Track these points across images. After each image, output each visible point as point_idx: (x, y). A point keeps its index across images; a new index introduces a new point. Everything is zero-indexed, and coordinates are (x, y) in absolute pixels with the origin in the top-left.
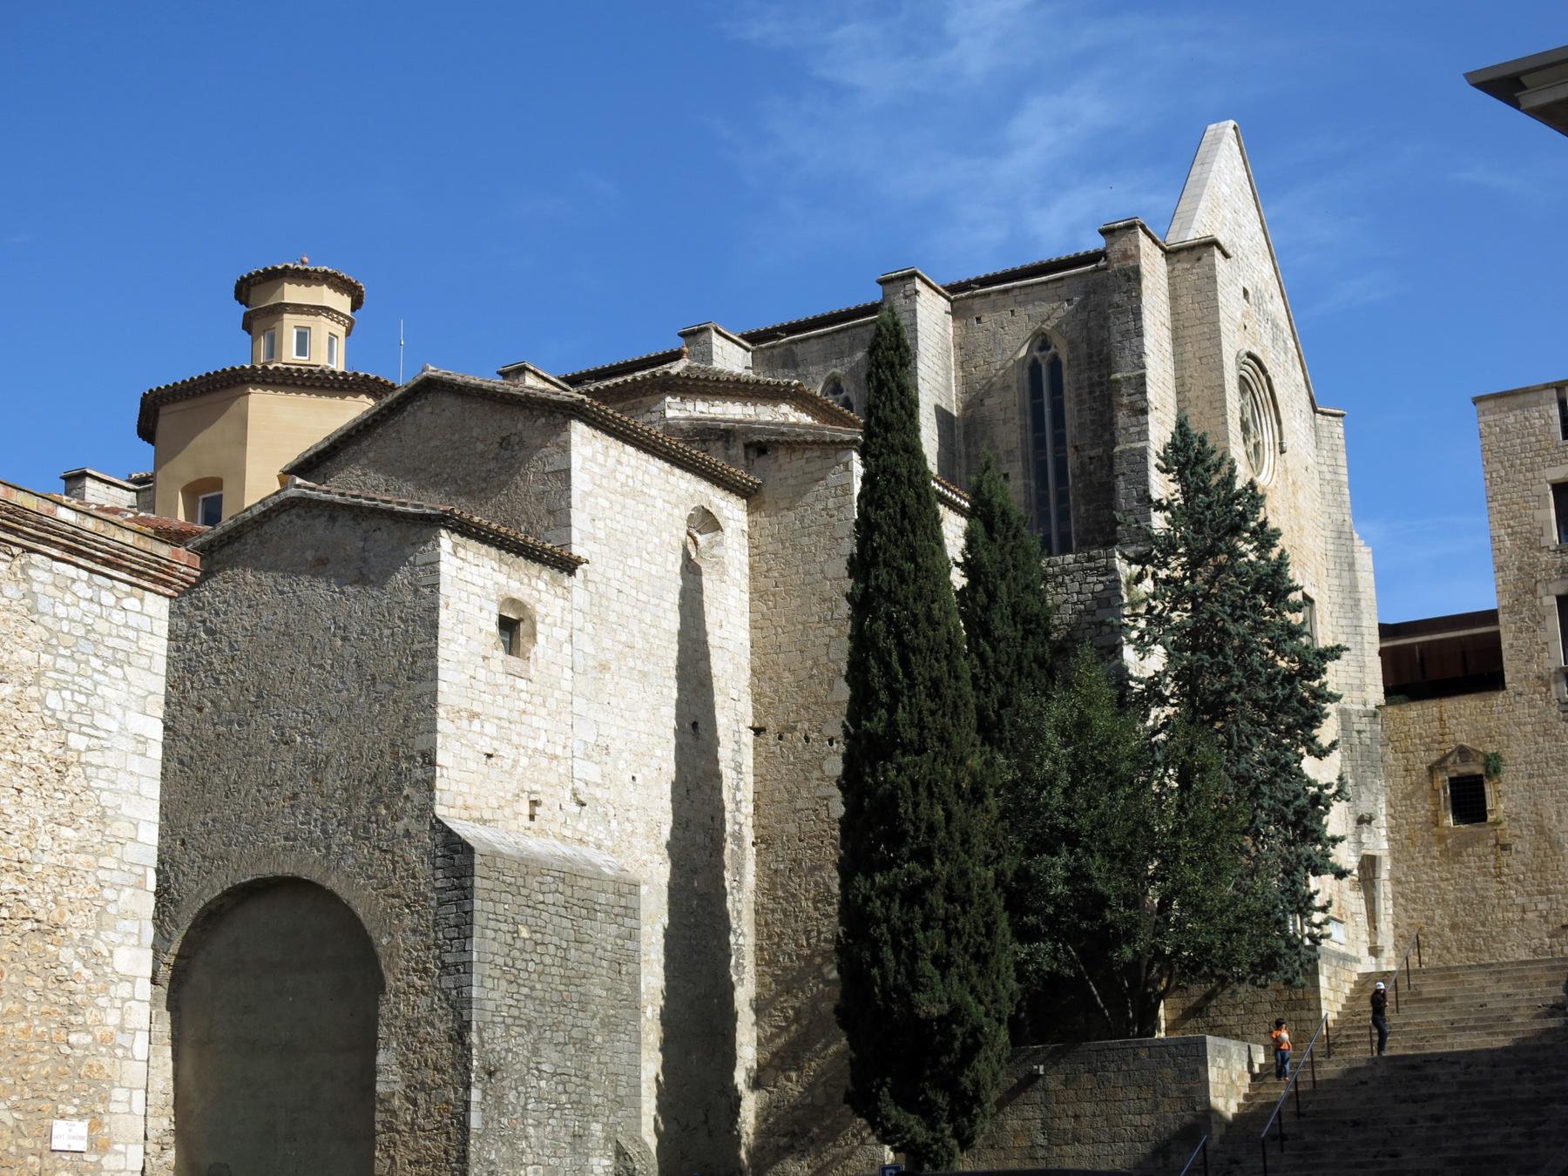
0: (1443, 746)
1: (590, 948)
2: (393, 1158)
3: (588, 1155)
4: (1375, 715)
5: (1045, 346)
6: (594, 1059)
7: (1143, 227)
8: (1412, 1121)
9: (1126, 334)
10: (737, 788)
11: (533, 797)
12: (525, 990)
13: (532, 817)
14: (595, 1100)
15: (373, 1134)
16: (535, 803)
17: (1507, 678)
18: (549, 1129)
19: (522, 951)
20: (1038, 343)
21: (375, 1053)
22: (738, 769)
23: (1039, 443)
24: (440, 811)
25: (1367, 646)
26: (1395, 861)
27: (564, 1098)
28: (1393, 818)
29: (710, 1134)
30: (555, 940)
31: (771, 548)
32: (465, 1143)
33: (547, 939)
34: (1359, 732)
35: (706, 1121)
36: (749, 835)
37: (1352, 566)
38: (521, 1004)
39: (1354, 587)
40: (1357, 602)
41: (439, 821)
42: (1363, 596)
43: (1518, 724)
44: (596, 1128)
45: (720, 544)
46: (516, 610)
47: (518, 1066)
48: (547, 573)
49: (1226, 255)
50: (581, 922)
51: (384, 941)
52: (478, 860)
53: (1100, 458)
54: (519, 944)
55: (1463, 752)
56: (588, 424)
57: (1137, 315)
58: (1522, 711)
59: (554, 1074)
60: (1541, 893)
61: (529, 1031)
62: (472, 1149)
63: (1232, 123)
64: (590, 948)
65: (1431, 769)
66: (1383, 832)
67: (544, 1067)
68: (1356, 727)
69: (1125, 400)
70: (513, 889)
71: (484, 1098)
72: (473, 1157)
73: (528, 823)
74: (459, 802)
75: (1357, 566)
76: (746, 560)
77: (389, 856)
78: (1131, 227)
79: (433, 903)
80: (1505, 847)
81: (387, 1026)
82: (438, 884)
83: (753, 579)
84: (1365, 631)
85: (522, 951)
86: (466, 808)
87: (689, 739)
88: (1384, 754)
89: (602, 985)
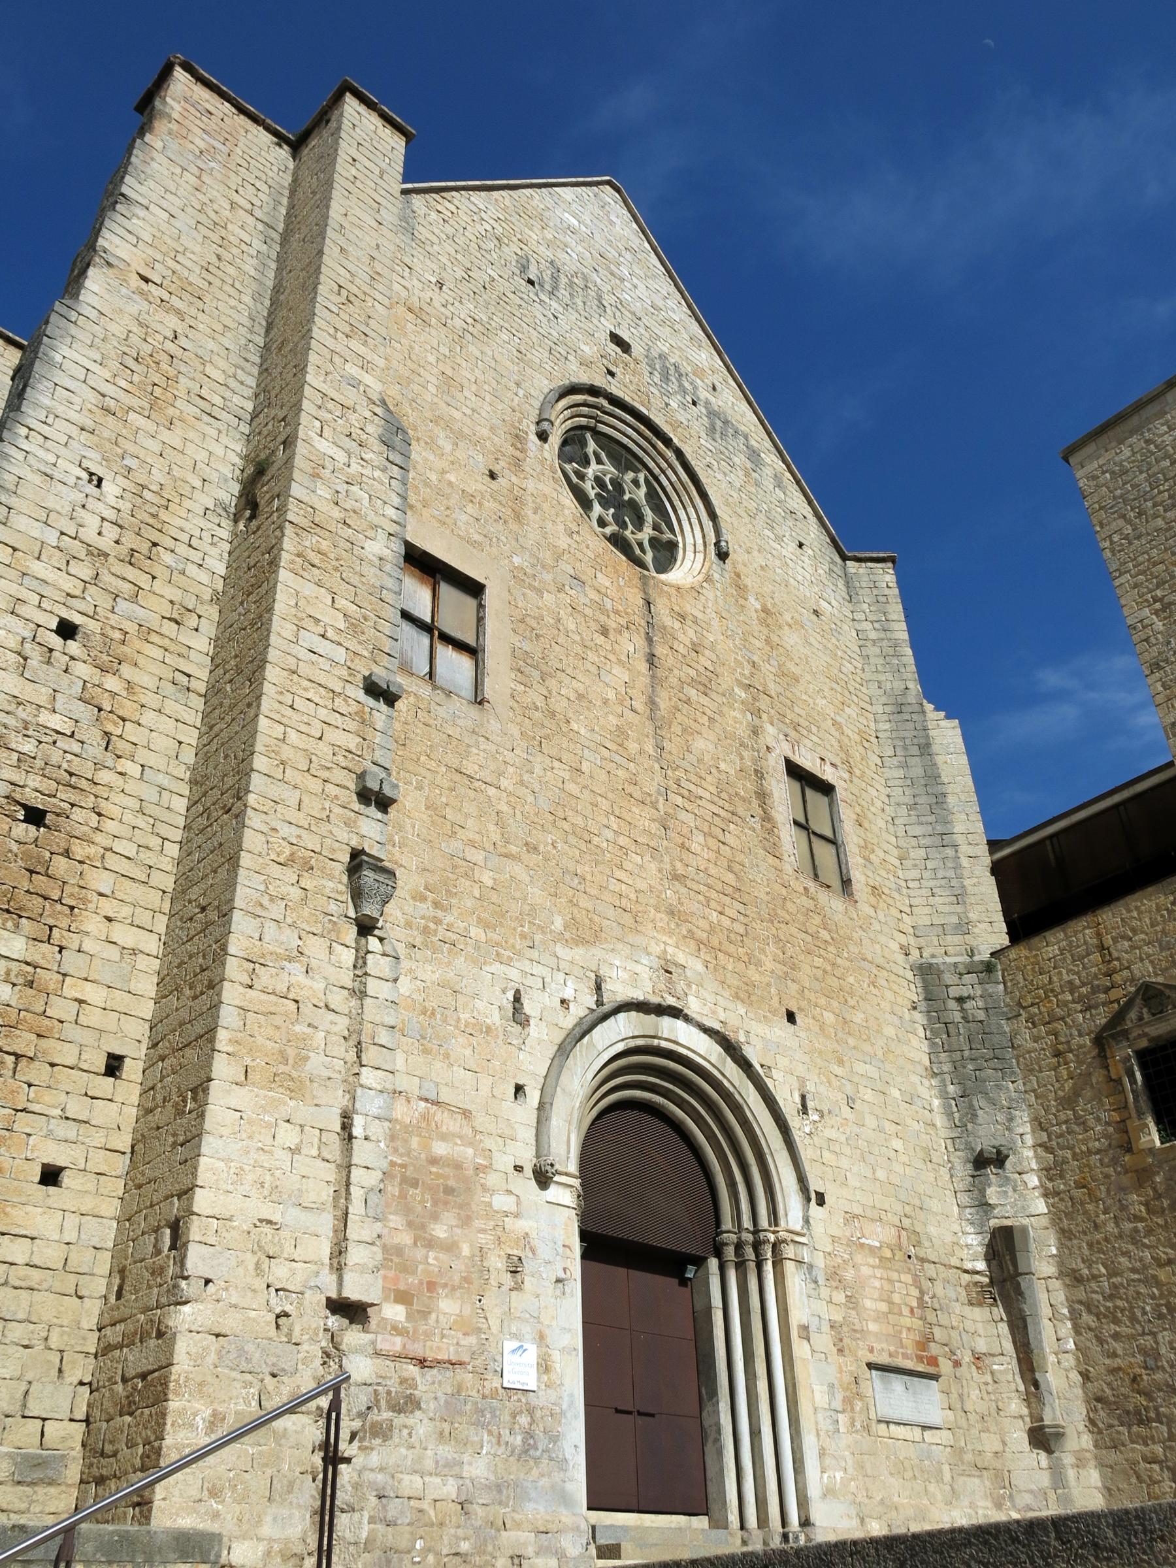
0: (1115, 994)
4: (989, 968)
25: (965, 862)
26: (1065, 1235)
28: (1048, 1149)
34: (960, 1000)
37: (925, 749)
39: (932, 777)
40: (940, 800)
42: (949, 789)
66: (1033, 1180)
68: (954, 992)
75: (935, 748)
84: (960, 839)
88: (1015, 1033)
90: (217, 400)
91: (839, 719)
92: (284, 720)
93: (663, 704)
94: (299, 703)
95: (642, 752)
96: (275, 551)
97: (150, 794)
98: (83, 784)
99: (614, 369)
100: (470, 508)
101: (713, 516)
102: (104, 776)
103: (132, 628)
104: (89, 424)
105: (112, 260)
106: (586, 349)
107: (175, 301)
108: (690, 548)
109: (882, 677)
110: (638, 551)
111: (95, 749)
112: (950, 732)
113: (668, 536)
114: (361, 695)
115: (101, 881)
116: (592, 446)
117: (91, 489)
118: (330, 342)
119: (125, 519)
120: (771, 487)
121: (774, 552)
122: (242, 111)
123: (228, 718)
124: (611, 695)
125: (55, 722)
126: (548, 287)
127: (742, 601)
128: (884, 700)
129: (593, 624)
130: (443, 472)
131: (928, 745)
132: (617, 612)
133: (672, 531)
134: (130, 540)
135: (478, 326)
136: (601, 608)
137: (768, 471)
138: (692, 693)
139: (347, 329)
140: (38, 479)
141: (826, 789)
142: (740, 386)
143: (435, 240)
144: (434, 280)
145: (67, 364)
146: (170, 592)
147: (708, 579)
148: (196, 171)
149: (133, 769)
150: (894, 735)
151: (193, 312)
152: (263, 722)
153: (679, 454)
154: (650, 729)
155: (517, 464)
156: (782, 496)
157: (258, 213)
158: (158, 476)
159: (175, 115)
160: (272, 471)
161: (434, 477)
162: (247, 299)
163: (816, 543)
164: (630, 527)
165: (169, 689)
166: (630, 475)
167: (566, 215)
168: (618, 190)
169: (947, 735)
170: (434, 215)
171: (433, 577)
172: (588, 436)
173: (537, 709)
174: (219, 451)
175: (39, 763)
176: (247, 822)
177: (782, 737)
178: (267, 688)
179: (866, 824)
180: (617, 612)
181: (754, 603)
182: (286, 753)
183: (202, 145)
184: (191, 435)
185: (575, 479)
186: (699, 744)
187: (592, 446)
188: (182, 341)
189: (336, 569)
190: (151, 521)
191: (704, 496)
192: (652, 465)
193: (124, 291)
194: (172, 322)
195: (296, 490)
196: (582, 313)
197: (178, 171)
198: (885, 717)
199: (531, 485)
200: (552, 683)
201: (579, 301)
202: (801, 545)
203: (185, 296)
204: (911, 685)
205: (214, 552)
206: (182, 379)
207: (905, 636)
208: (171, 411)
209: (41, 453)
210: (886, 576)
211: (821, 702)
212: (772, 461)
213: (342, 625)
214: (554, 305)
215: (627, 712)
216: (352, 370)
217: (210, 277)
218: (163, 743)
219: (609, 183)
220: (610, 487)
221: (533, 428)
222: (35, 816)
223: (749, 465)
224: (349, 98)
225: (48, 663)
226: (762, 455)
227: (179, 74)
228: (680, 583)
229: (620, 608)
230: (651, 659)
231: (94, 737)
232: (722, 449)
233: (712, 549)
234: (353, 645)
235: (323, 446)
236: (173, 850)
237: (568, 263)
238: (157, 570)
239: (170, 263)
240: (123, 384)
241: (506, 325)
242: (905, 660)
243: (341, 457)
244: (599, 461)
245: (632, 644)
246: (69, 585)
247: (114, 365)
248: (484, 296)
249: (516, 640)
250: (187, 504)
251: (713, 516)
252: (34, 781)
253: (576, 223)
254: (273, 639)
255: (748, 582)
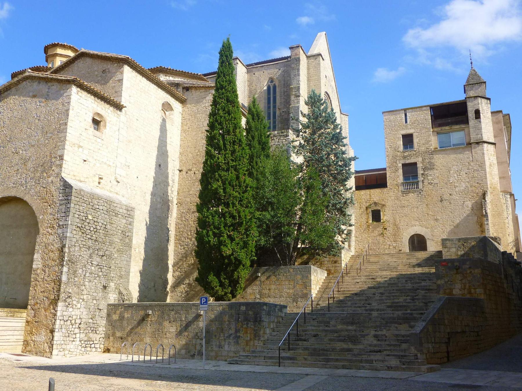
1: (115, 226)
2: (36, 290)
3: (108, 293)
5: (272, 82)
6: (113, 262)
7: (301, 47)
8: (374, 294)
9: (295, 75)
10: (172, 187)
11: (100, 177)
12: (89, 236)
13: (99, 183)
14: (113, 275)
15: (30, 281)
16: (100, 178)
17: (388, 185)
18: (94, 283)
19: (89, 223)
20: (270, 81)
21: (33, 254)
22: (173, 181)
23: (269, 108)
24: (63, 175)
26: (356, 231)
27: (100, 274)
29: (155, 290)
30: (102, 221)
31: (188, 118)
32: (60, 285)
33: (99, 221)
35: (154, 287)
36: (175, 202)
38: (87, 241)
41: (62, 178)
43: (390, 197)
44: (112, 285)
45: (172, 114)
46: (100, 118)
47: (84, 261)
48: (112, 108)
49: (323, 60)
50: (112, 217)
51: (41, 217)
52: (74, 191)
53: (286, 112)
54: (88, 221)
55: (375, 204)
56: (131, 68)
57: (298, 70)
58: (391, 194)
59: (98, 265)
60: (394, 241)
61: (89, 250)
62: (62, 288)
63: (325, 33)
64: (115, 226)
65: (367, 208)
67: (93, 263)
69: (294, 93)
70: (87, 202)
71: (69, 271)
72: (62, 290)
73: (97, 185)
74: (72, 173)
76: (181, 121)
77: (45, 189)
78: (298, 47)
79: (58, 205)
80: (385, 229)
81: (39, 245)
82: (60, 199)
83: (182, 126)
85: (89, 223)
86: (74, 176)
87: (158, 169)
89: (118, 238)
153: (331, 101)
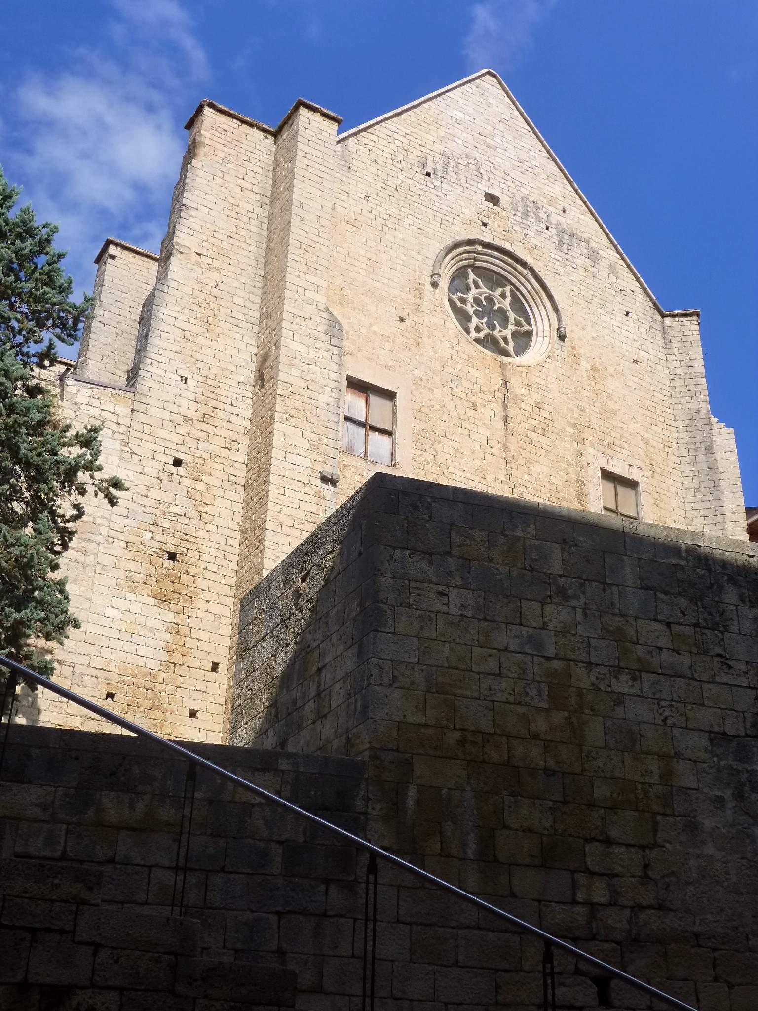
25: (729, 525)
37: (709, 450)
39: (712, 469)
42: (723, 476)
75: (716, 449)
84: (727, 510)
90: (241, 317)
91: (647, 435)
92: (281, 502)
93: (513, 447)
94: (288, 492)
95: (496, 479)
96: (272, 411)
97: (221, 540)
98: (192, 539)
99: (486, 221)
100: (388, 346)
101: (556, 310)
102: (200, 534)
103: (206, 456)
104: (178, 349)
105: (181, 249)
106: (467, 211)
107: (216, 263)
108: (541, 334)
109: (683, 401)
110: (503, 344)
111: (195, 522)
112: (728, 437)
113: (526, 327)
114: (318, 482)
115: (202, 584)
116: (472, 276)
117: (182, 385)
118: (296, 281)
119: (200, 398)
120: (606, 275)
121: (604, 324)
122: (243, 122)
123: (255, 500)
124: (477, 447)
125: (177, 510)
126: (440, 174)
127: (575, 366)
128: (684, 417)
129: (466, 404)
130: (371, 326)
131: (711, 447)
132: (483, 392)
133: (529, 323)
134: (203, 409)
135: (393, 219)
136: (473, 392)
137: (604, 264)
138: (534, 436)
139: (305, 269)
140: (157, 386)
141: (633, 485)
142: (585, 203)
143: (364, 166)
144: (363, 196)
145: (166, 318)
146: (226, 434)
147: (551, 355)
148: (220, 174)
149: (213, 528)
150: (689, 441)
151: (225, 266)
152: (270, 504)
153: (532, 271)
154: (503, 465)
155: (418, 309)
156: (615, 279)
157: (256, 189)
158: (214, 370)
159: (207, 141)
160: (271, 359)
161: (364, 331)
162: (253, 248)
163: (640, 310)
164: (498, 328)
165: (226, 485)
166: (500, 290)
167: (455, 112)
168: (494, 76)
169: (725, 439)
170: (362, 148)
171: (366, 393)
172: (470, 271)
173: (428, 463)
174: (242, 346)
175: (172, 531)
176: (265, 555)
177: (600, 455)
178: (272, 487)
179: (661, 505)
180: (483, 392)
181: (585, 365)
182: (282, 518)
183: (222, 155)
184: (229, 341)
185: (459, 304)
186: (537, 469)
187: (472, 276)
188: (221, 286)
189: (304, 416)
190: (212, 396)
191: (550, 297)
192: (514, 280)
193: (189, 265)
194: (215, 276)
195: (281, 376)
196: (464, 185)
197: (211, 178)
198: (684, 429)
199: (426, 320)
200: (438, 446)
201: (462, 177)
202: (627, 314)
203: (220, 257)
204: (703, 405)
205: (244, 406)
206: (222, 309)
207: (703, 370)
208: (218, 330)
209: (157, 371)
210: (692, 326)
211: (633, 426)
212: (609, 255)
213: (308, 446)
214: (444, 186)
215: (488, 457)
216: (310, 294)
217: (232, 241)
218: (225, 513)
219: (488, 73)
220: (484, 303)
221: (428, 280)
222: (172, 556)
223: (589, 262)
224: (303, 111)
225: (171, 481)
226: (601, 252)
227: (207, 111)
228: (529, 363)
229: (485, 389)
230: (506, 419)
231: (194, 514)
232: (567, 256)
233: (555, 333)
234: (313, 456)
235: (295, 346)
236: (234, 566)
237: (455, 148)
238: (217, 422)
239: (212, 240)
240: (192, 321)
241: (411, 212)
242: (700, 387)
243: (304, 349)
244: (477, 286)
245: (494, 412)
246: (177, 439)
247: (187, 311)
248: (396, 196)
249: (415, 423)
250: (229, 381)
251: (556, 310)
252: (170, 540)
253: (462, 115)
254: (273, 461)
255: (581, 351)
